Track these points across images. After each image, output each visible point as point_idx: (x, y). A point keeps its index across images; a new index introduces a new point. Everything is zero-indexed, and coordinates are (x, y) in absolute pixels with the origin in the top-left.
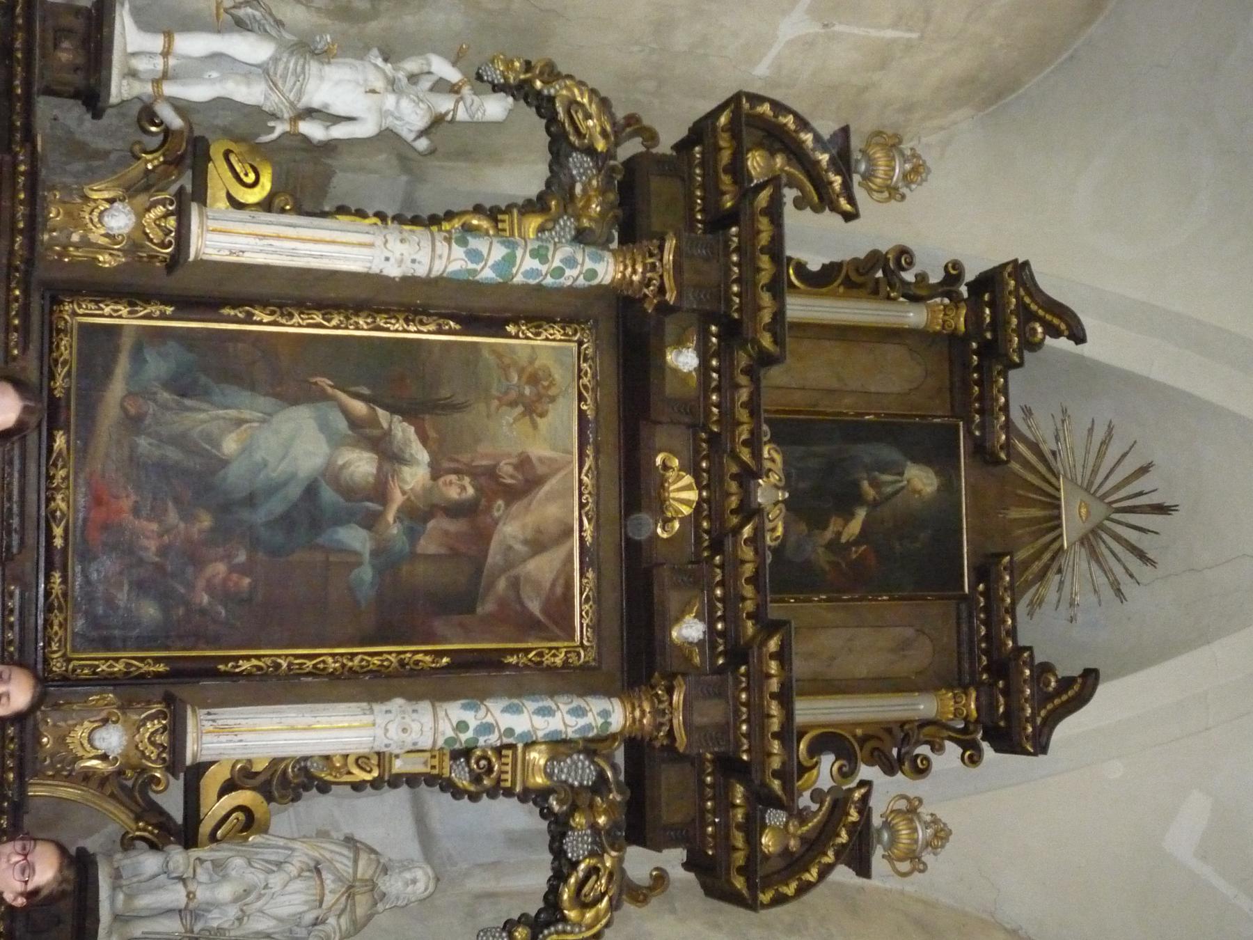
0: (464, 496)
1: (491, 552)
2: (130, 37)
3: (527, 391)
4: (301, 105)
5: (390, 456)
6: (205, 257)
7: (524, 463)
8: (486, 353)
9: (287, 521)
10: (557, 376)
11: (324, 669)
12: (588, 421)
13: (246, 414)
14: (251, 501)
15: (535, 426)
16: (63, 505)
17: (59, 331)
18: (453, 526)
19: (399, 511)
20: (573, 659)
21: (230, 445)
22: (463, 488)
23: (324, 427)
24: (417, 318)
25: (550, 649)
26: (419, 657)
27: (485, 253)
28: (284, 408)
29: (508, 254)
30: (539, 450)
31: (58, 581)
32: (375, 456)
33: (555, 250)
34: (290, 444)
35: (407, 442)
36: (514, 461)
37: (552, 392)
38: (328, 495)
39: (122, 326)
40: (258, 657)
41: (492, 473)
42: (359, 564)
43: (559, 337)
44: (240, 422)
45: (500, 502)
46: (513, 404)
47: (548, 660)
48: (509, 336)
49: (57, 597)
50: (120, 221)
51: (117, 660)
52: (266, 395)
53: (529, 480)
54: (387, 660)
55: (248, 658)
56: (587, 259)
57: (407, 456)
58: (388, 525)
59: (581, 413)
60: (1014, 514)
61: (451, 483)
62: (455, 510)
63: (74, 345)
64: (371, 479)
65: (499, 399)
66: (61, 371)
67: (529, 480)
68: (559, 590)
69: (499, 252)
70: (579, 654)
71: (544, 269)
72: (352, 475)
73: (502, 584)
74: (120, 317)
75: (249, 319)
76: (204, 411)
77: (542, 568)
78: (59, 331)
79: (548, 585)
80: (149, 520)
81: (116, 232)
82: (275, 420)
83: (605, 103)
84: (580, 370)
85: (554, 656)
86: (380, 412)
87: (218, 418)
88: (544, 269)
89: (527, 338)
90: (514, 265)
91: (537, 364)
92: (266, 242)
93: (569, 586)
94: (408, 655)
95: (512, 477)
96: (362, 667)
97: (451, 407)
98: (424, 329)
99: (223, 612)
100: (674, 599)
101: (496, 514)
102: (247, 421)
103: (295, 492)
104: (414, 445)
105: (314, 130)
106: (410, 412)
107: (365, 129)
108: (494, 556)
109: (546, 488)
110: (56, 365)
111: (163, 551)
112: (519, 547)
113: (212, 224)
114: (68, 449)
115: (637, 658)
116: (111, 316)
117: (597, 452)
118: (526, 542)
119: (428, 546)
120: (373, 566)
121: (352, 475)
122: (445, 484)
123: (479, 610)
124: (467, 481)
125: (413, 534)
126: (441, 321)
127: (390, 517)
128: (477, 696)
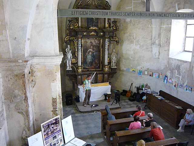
2: (68, 69)
4: (70, 58)
5: (90, 51)
7: (90, 43)
9: (94, 58)
18: (94, 47)
21: (89, 61)
23: (89, 55)
30: (89, 42)
34: (89, 58)
38: (92, 55)
50: (80, 70)
53: (91, 42)
60: (93, 4)
62: (93, 48)
67: (91, 42)
77: (97, 42)
83: (66, 37)
97: (87, 47)
100: (99, 34)
105: (72, 58)
107: (71, 54)
108: (96, 45)
115: (103, 37)
125: (95, 50)
128: (105, 49)
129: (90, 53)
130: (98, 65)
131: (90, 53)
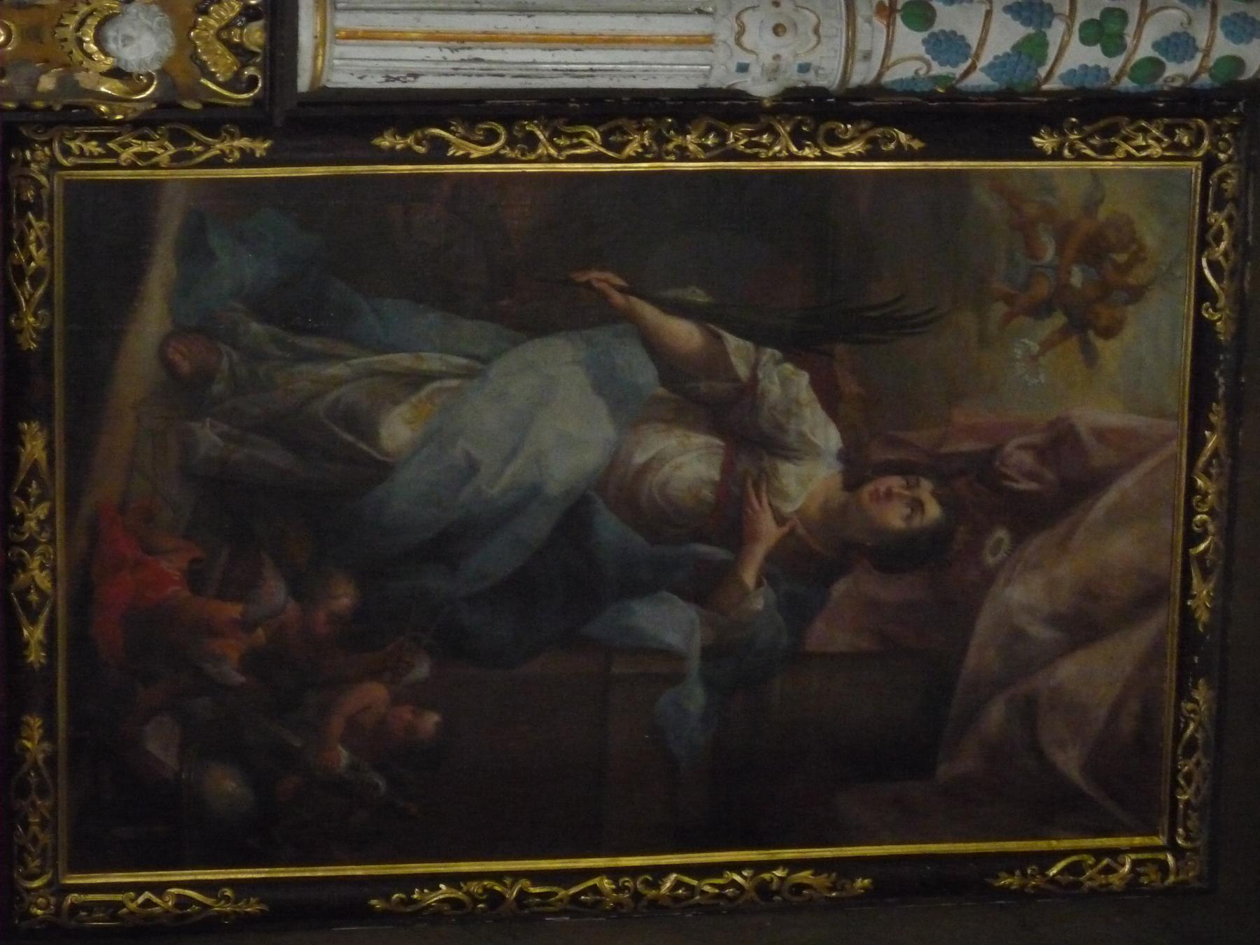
0: (917, 522)
1: (975, 641)
3: (1077, 278)
5: (752, 438)
6: (330, 85)
7: (1060, 442)
8: (983, 196)
10: (1150, 241)
11: (596, 904)
12: (1218, 347)
13: (432, 361)
14: (446, 545)
15: (1090, 356)
16: (42, 579)
17: (25, 206)
19: (769, 558)
20: (1150, 877)
21: (397, 429)
22: (917, 505)
23: (606, 384)
24: (823, 128)
25: (1099, 853)
26: (805, 876)
27: (973, 41)
28: (515, 344)
29: (1028, 39)
30: (1096, 413)
31: (37, 734)
32: (717, 442)
33: (1144, 16)
35: (792, 407)
36: (1036, 438)
37: (1138, 275)
38: (609, 527)
39: (156, 184)
40: (454, 880)
41: (984, 468)
42: (676, 678)
43: (1156, 150)
44: (415, 380)
45: (1001, 534)
46: (1041, 310)
47: (1092, 878)
48: (1040, 155)
49: (35, 767)
51: (160, 888)
52: (477, 315)
54: (734, 883)
55: (431, 881)
56: (1220, 33)
57: (791, 439)
58: (745, 593)
59: (1202, 328)
61: (889, 495)
62: (898, 554)
63: (59, 235)
64: (707, 493)
65: (1008, 299)
66: (28, 294)
68: (1127, 725)
69: (1006, 35)
70: (1163, 866)
71: (1114, 65)
72: (665, 484)
73: (996, 713)
74: (156, 166)
75: (439, 151)
76: (340, 358)
77: (1095, 676)
78: (25, 206)
79: (1102, 713)
80: (221, 596)
81: (133, 68)
82: (496, 370)
84: (1204, 227)
85: (1108, 870)
86: (732, 341)
87: (373, 373)
88: (1114, 65)
89: (1082, 157)
90: (1041, 63)
91: (1103, 213)
92: (465, 54)
93: (1148, 715)
94: (779, 873)
95: (1031, 476)
96: (677, 899)
98: (836, 152)
99: (382, 783)
101: (990, 560)
102: (429, 377)
103: (537, 526)
104: (807, 412)
106: (800, 345)
108: (981, 654)
109: (1111, 496)
110: (20, 279)
111: (254, 661)
112: (1040, 632)
113: (343, 21)
114: (51, 461)
116: (133, 166)
117: (1235, 410)
118: (1054, 620)
119: (831, 633)
120: (709, 684)
121: (665, 484)
122: (876, 497)
123: (944, 771)
124: (926, 488)
125: (798, 612)
126: (878, 133)
127: (749, 576)
129: (687, 461)
130: (226, 785)
131: (687, 461)
